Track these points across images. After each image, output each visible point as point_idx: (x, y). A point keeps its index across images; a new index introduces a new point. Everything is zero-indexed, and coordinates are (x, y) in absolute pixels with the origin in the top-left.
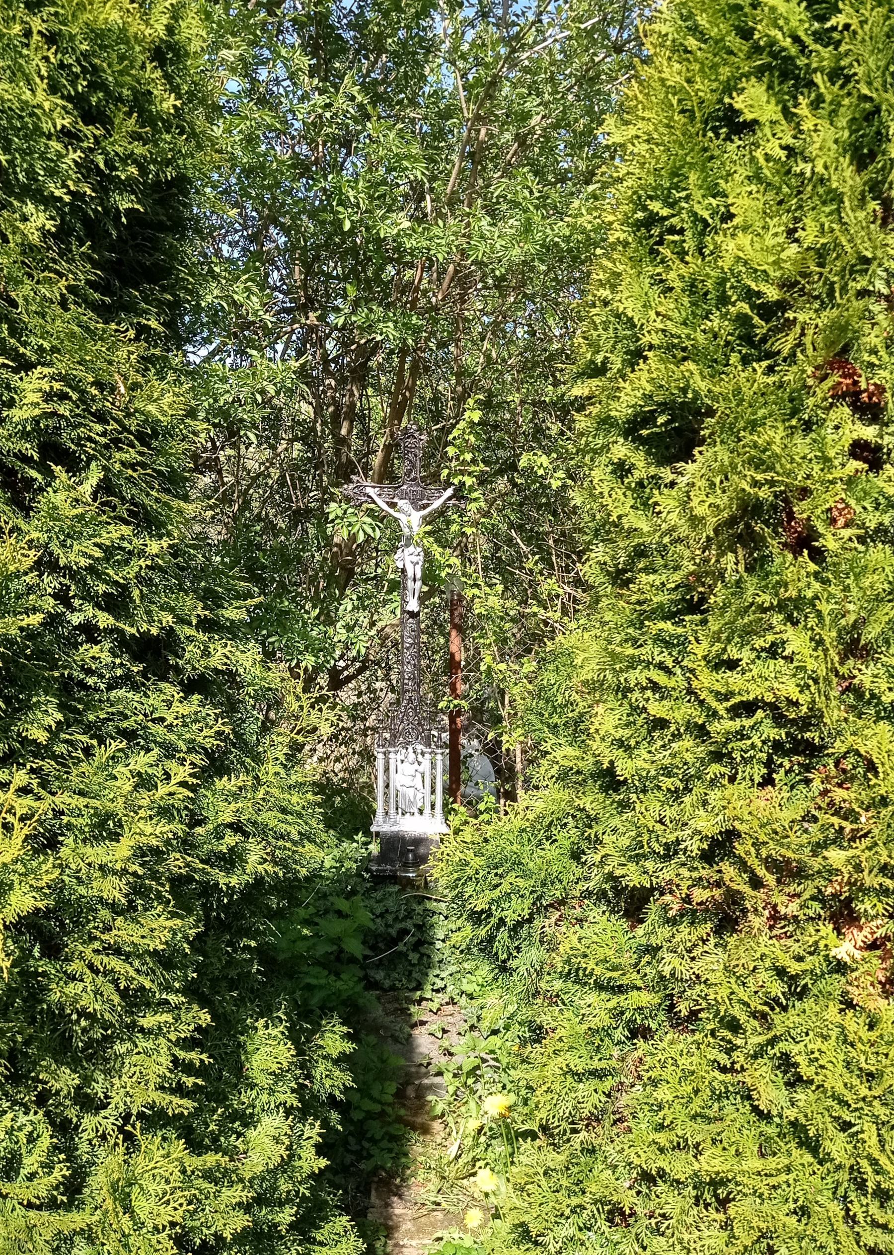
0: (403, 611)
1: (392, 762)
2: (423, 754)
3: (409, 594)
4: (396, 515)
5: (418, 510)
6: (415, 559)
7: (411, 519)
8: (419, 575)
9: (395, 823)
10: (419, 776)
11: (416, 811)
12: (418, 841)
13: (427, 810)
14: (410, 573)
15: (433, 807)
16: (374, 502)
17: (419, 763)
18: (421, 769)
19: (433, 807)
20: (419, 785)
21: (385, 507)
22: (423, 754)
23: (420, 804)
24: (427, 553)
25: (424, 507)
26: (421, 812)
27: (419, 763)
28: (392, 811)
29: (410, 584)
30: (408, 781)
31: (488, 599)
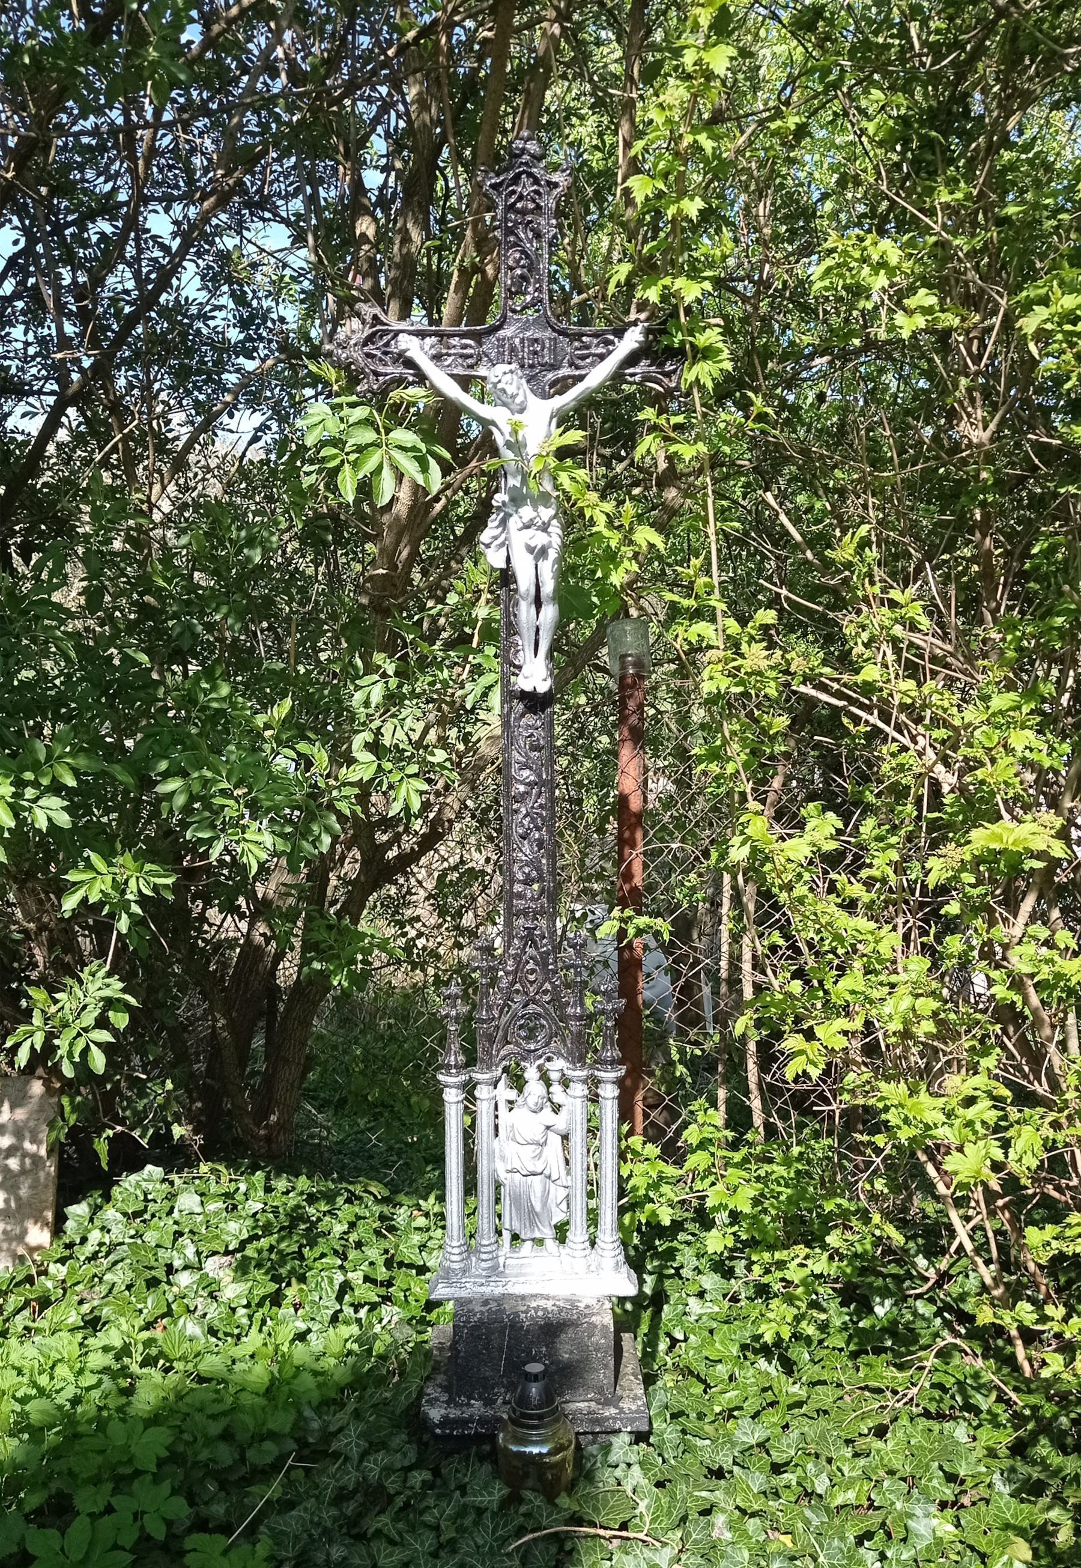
0: (511, 695)
1: (484, 1109)
2: (565, 1083)
3: (525, 642)
4: (485, 411)
5: (546, 396)
6: (539, 539)
7: (529, 422)
8: (548, 587)
9: (495, 1271)
10: (555, 1141)
11: (548, 1233)
12: (553, 1328)
13: (578, 1234)
14: (525, 582)
15: (593, 1218)
16: (421, 378)
17: (557, 1109)
18: (560, 1122)
19: (593, 1218)
20: (556, 1166)
21: (452, 390)
22: (565, 1083)
23: (558, 1217)
24: (572, 518)
25: (562, 386)
26: (561, 1232)
27: (557, 1109)
28: (487, 1239)
29: (525, 611)
30: (525, 1158)
31: (733, 656)
